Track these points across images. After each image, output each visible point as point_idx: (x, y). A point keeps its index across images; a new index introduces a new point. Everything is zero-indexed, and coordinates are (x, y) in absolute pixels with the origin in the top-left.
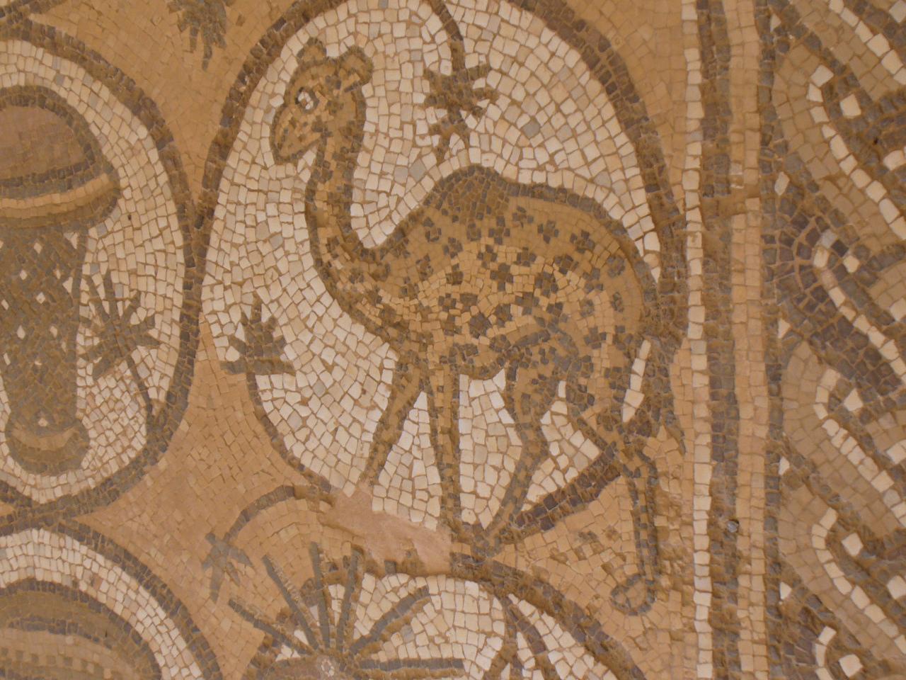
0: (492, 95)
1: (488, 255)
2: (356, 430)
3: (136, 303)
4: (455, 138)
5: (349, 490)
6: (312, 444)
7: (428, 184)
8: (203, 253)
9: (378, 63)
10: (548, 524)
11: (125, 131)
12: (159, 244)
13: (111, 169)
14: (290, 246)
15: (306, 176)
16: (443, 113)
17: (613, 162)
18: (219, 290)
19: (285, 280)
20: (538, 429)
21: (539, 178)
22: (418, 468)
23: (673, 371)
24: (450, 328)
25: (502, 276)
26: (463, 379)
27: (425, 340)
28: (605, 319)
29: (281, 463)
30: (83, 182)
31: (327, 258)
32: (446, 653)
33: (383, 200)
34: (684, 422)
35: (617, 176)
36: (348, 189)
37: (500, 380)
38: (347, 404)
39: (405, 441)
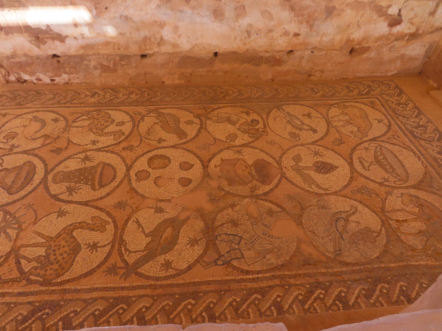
0: (92, 253)
1: (66, 252)
3: (76, 193)
4: (87, 246)
7: (81, 242)
8: (81, 204)
9: (103, 234)
10: (16, 263)
11: (105, 192)
12: (84, 197)
13: (99, 190)
15: (88, 222)
16: (91, 244)
18: (74, 207)
19: (72, 218)
20: (33, 261)
25: (61, 255)
26: (46, 248)
30: (98, 185)
31: (74, 225)
33: (80, 234)
36: (84, 229)
39: (39, 238)
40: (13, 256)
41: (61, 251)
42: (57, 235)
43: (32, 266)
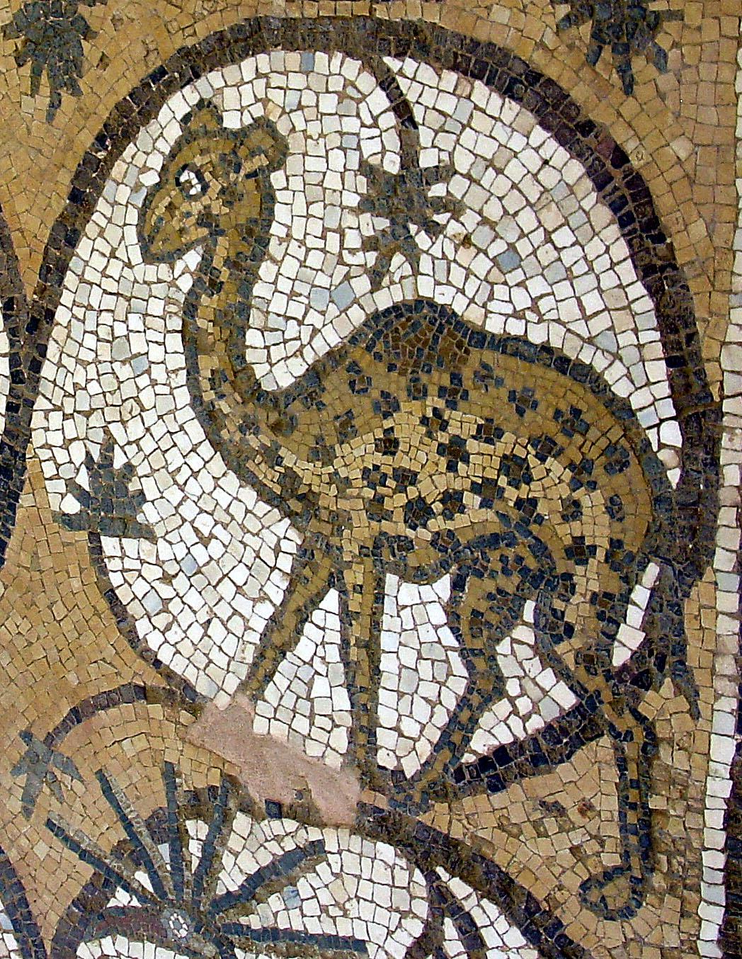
0: (454, 208)
1: (435, 422)
2: (236, 625)
5: (223, 701)
6: (173, 635)
8: (36, 367)
9: (295, 144)
10: (497, 785)
14: (158, 373)
15: (186, 283)
17: (623, 320)
18: (56, 417)
19: (150, 417)
20: (493, 658)
21: (516, 328)
22: (320, 687)
23: (689, 608)
24: (376, 509)
25: (455, 453)
26: (391, 580)
27: (339, 521)
28: (596, 527)
29: (129, 654)
31: (209, 396)
32: (344, 929)
33: (292, 329)
34: (700, 678)
35: (627, 339)
36: (245, 309)
37: (443, 586)
38: (227, 589)
39: (304, 649)
40: (439, 817)
41: (419, 453)
42: (289, 514)
43: (534, 666)
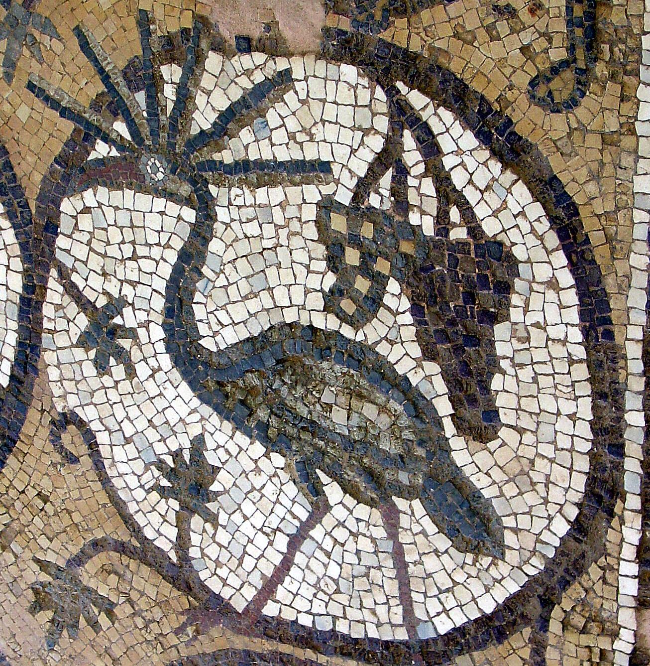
32: (311, 153)
